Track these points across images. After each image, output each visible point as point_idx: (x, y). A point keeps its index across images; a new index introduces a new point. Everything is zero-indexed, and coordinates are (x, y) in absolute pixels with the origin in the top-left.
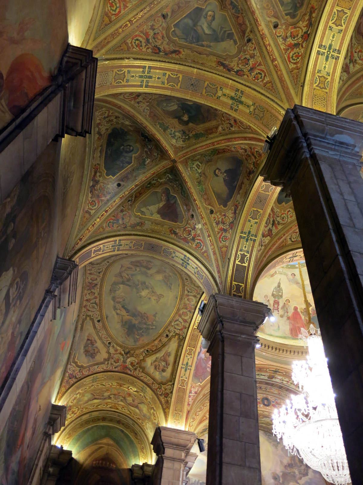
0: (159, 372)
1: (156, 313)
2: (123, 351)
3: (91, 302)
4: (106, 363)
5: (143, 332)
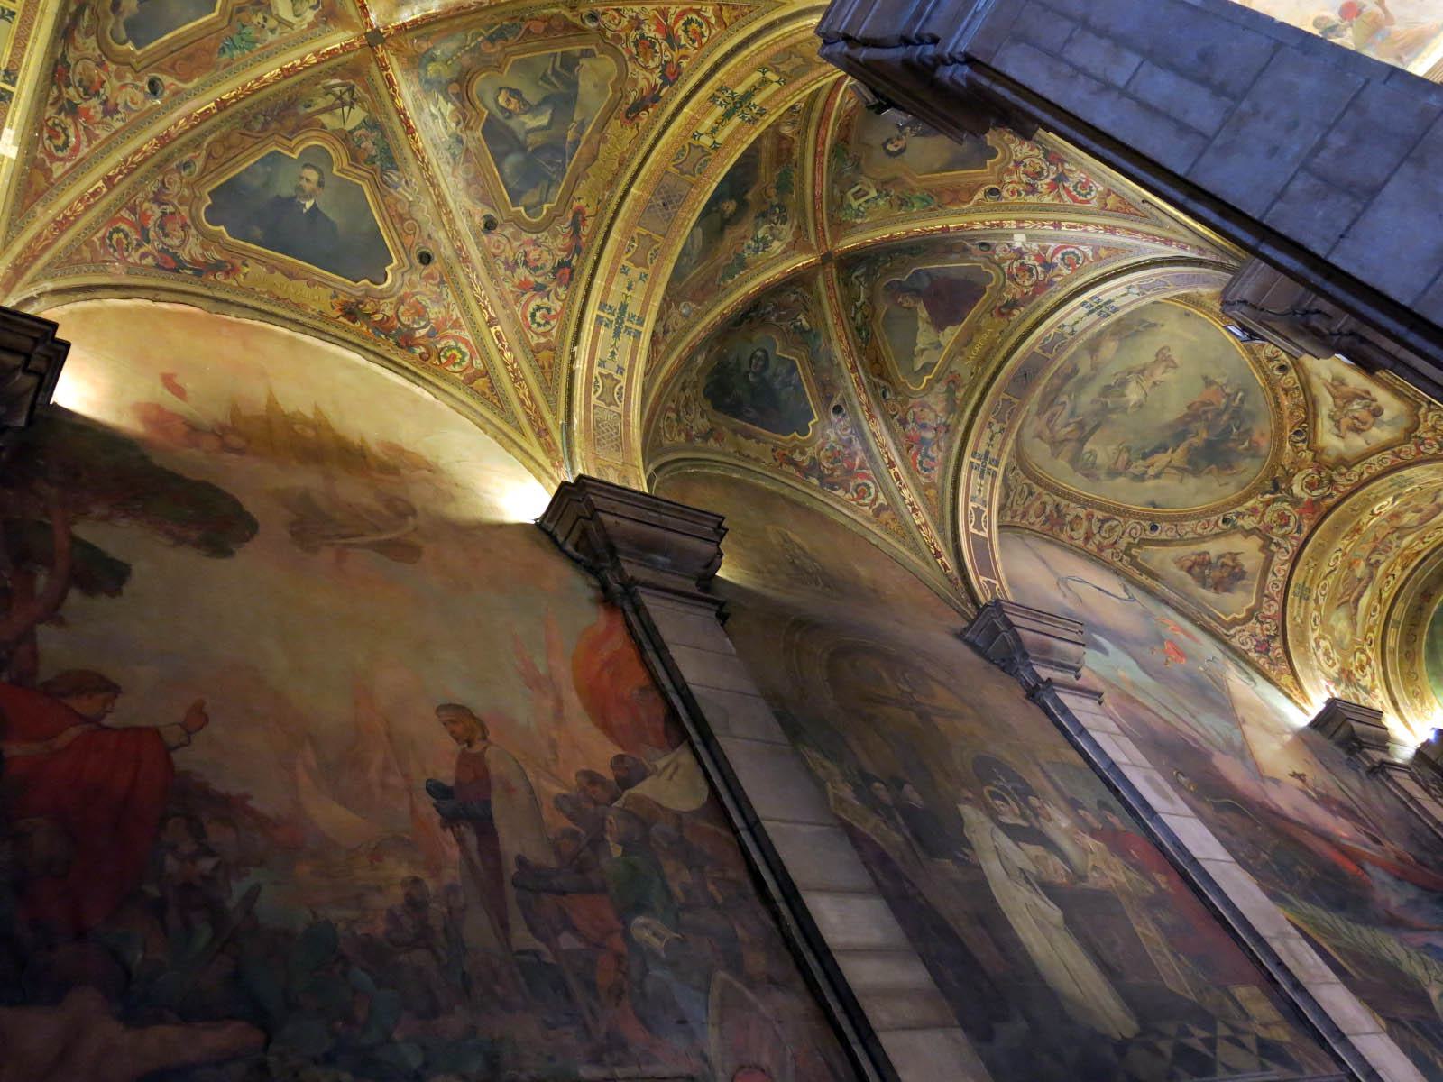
0: (1373, 425)
2: (1263, 494)
3: (1095, 530)
4: (1273, 548)
5: (1238, 428)
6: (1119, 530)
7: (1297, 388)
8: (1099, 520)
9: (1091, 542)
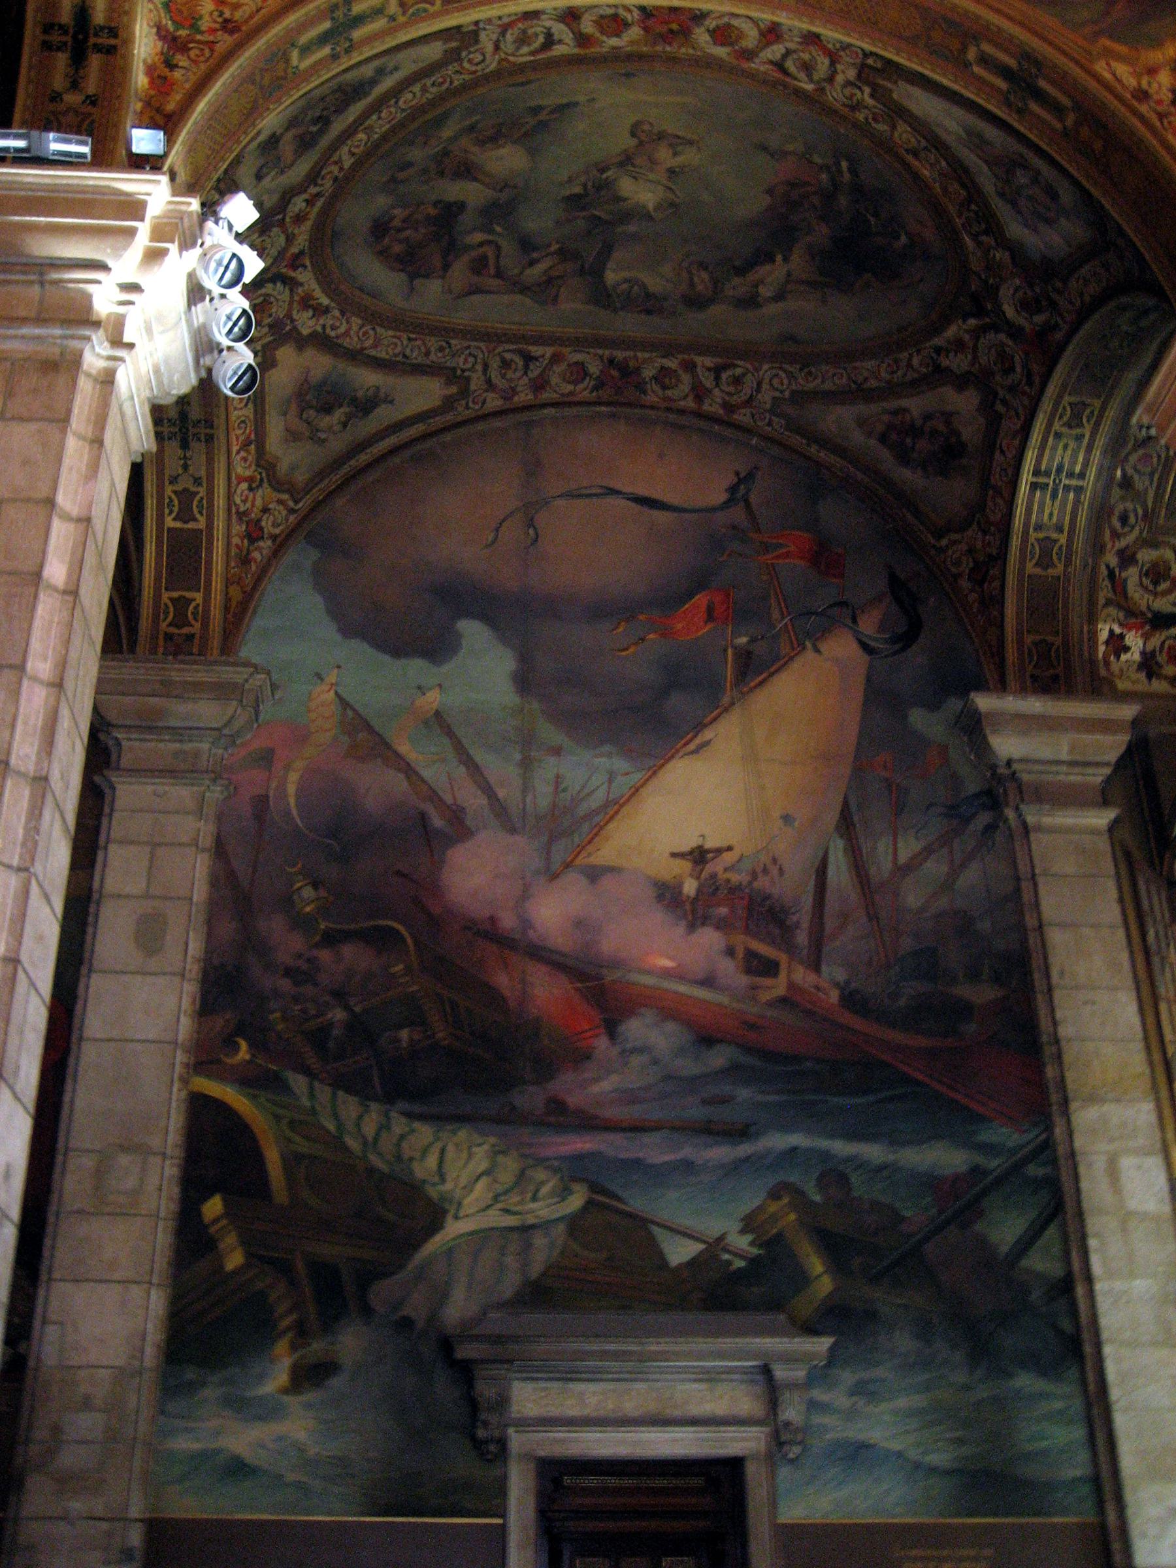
1: (764, 148)
3: (708, 383)
4: (1000, 408)
5: (876, 215)
7: (925, 148)
8: (709, 369)
9: (707, 401)
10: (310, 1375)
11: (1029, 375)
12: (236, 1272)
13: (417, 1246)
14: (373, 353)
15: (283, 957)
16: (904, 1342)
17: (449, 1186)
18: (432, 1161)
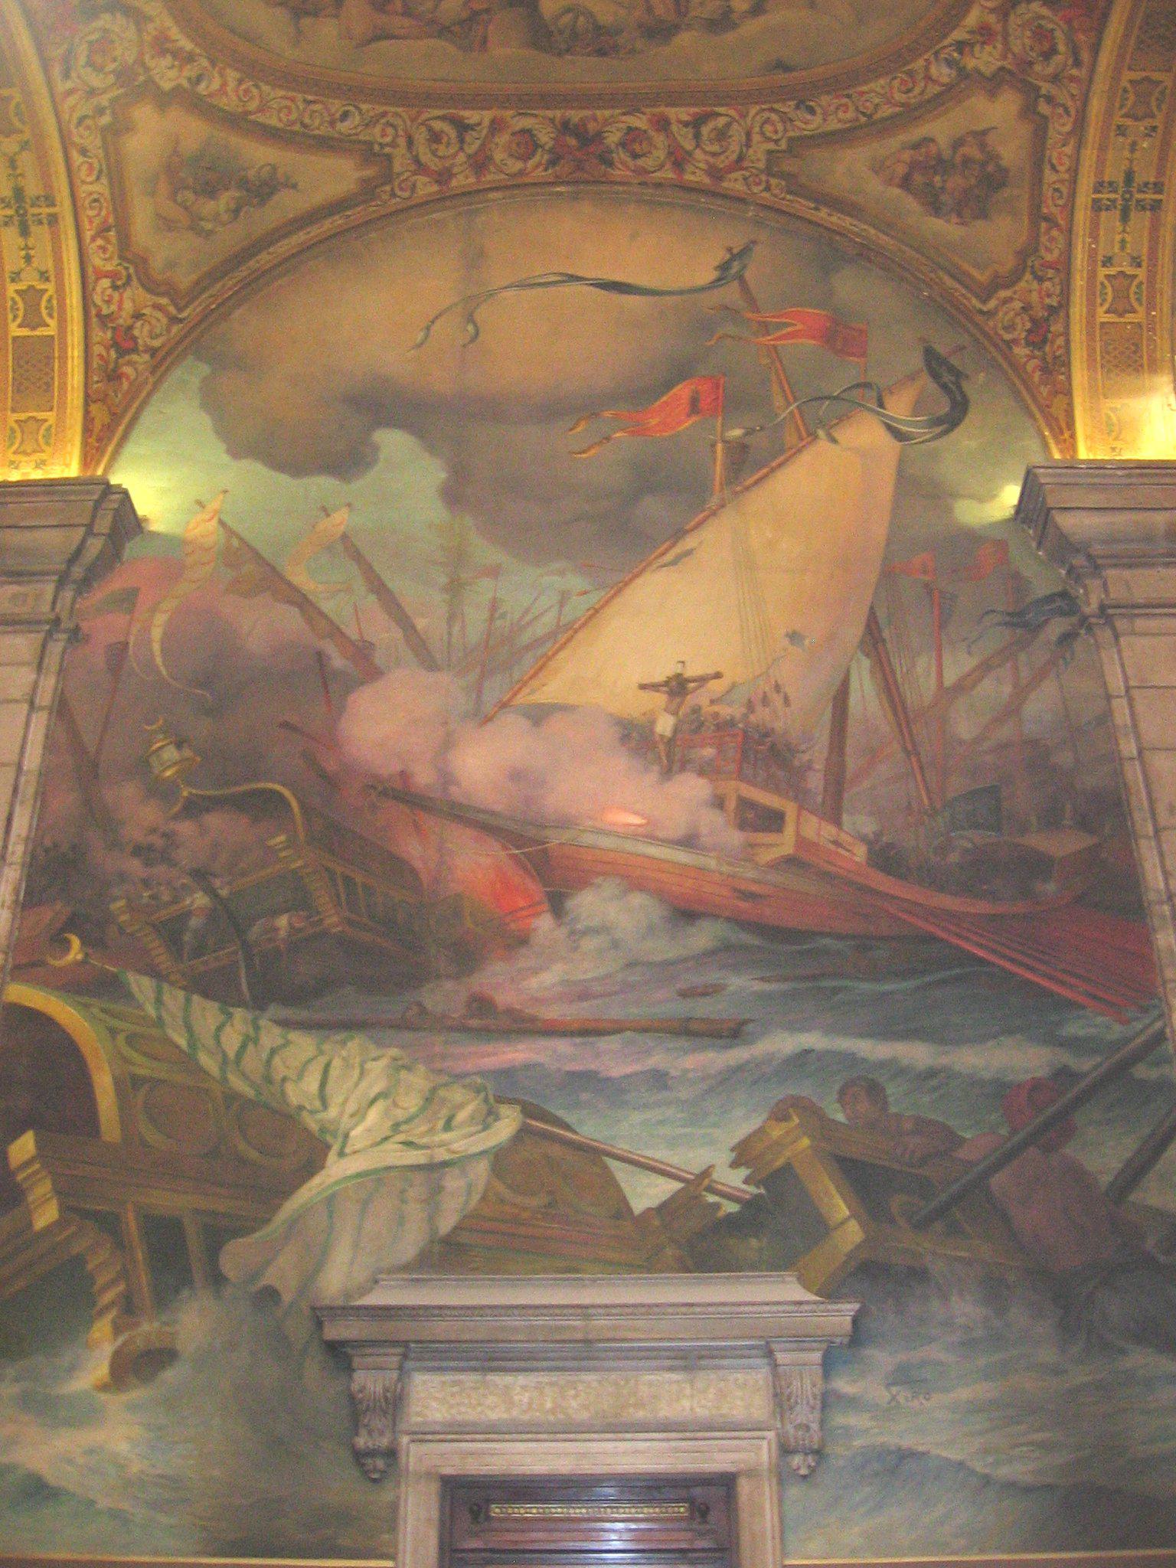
3: (688, 145)
4: (1044, 108)
6: (737, 133)
8: (686, 124)
9: (690, 168)
10: (136, 1366)
11: (1075, 52)
12: (49, 1230)
13: (287, 1192)
14: (260, 118)
15: (133, 833)
16: (966, 1309)
17: (333, 1112)
18: (312, 1083)
